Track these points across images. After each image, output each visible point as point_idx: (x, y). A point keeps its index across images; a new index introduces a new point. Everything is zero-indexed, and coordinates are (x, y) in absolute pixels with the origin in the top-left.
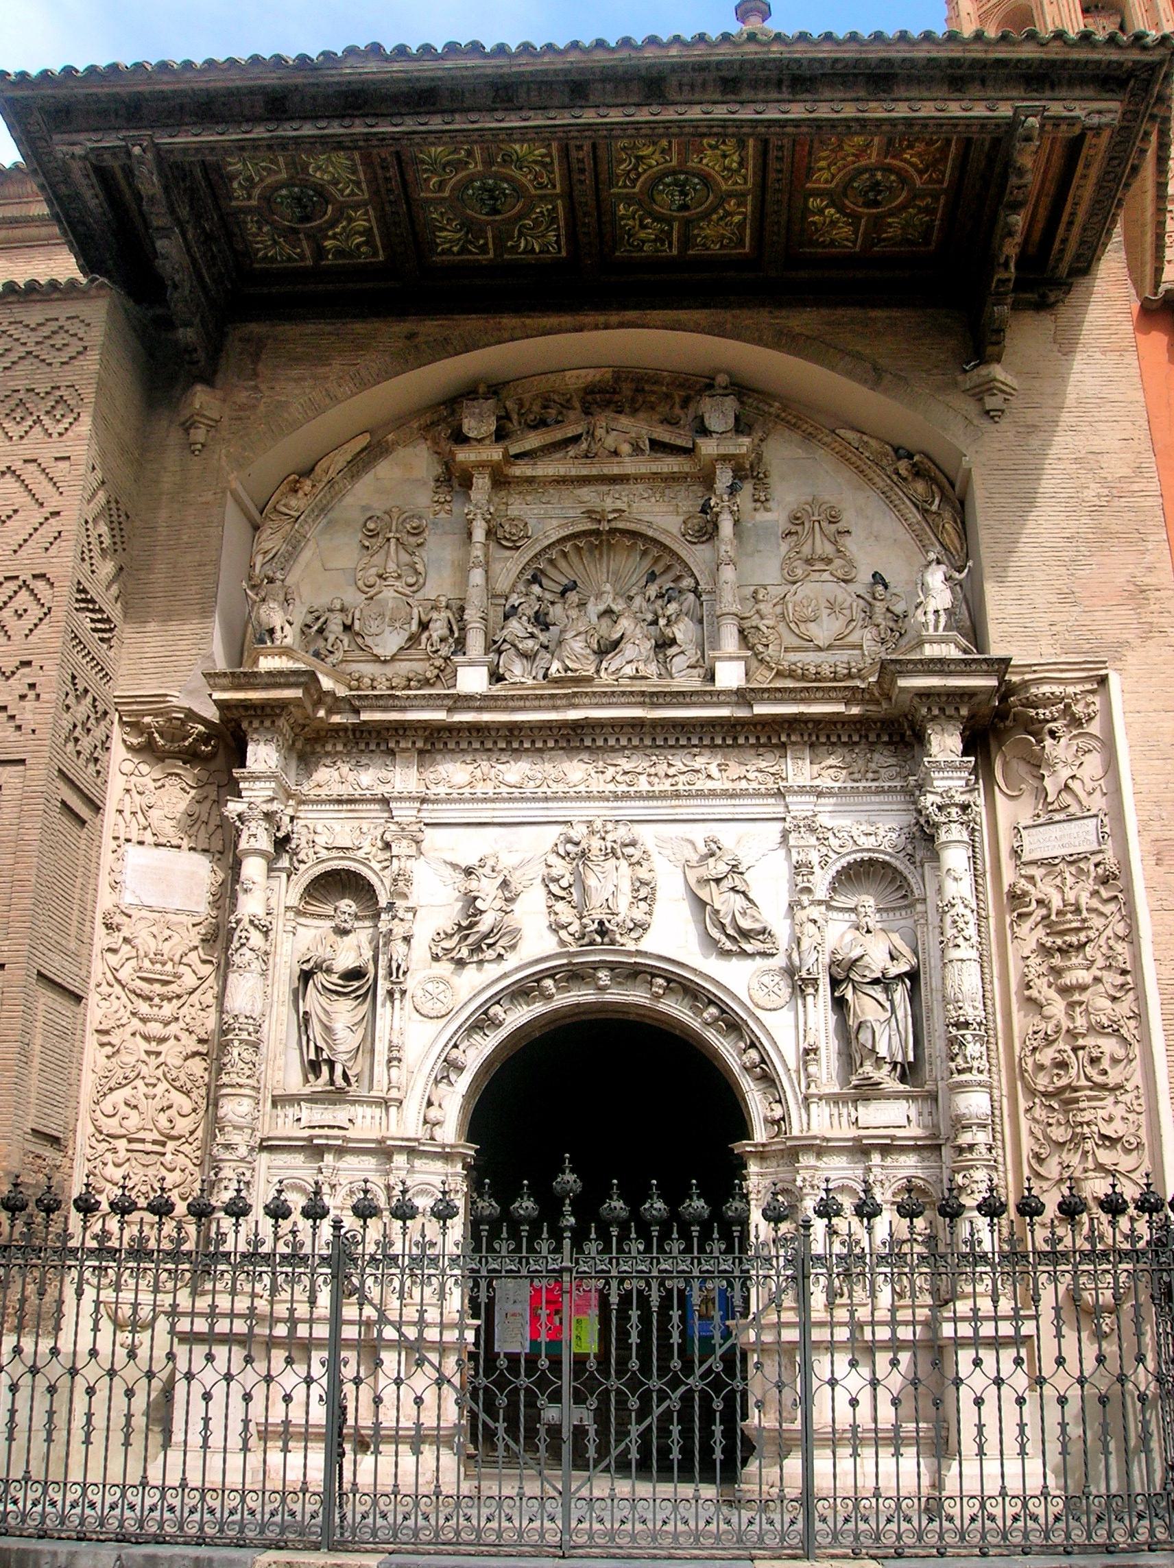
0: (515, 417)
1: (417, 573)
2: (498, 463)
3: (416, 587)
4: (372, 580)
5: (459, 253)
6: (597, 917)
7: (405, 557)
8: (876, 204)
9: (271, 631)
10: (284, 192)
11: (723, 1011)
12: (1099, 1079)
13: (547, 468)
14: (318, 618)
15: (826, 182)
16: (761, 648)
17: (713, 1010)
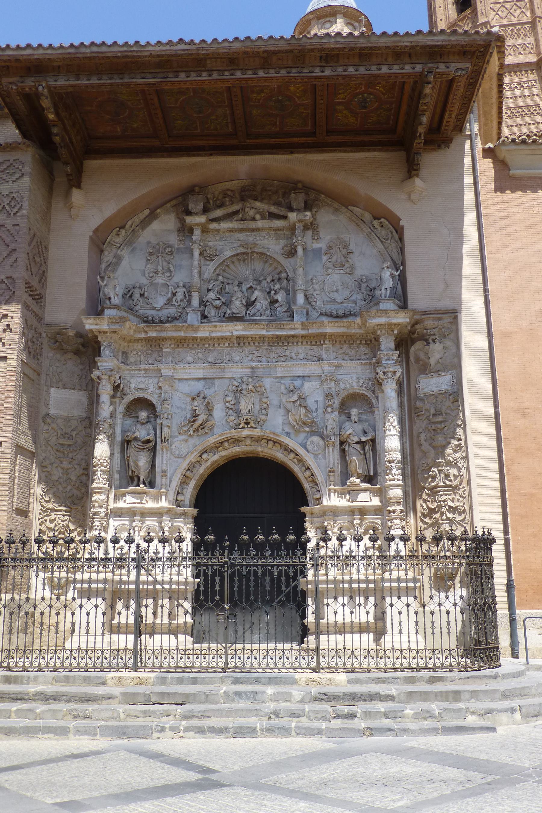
0: (211, 202)
1: (170, 271)
2: (204, 224)
3: (171, 277)
4: (151, 275)
6: (245, 417)
7: (165, 264)
8: (365, 107)
9: (110, 298)
11: (297, 455)
12: (448, 483)
13: (225, 225)
14: (129, 291)
15: (343, 99)
16: (314, 303)
17: (292, 455)
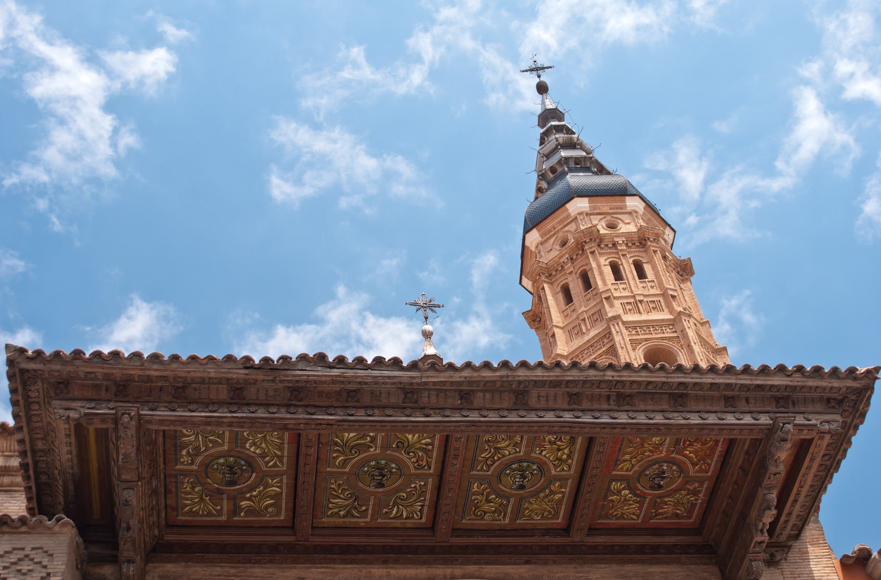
5: (344, 516)
8: (660, 487)
10: (222, 461)
15: (627, 470)
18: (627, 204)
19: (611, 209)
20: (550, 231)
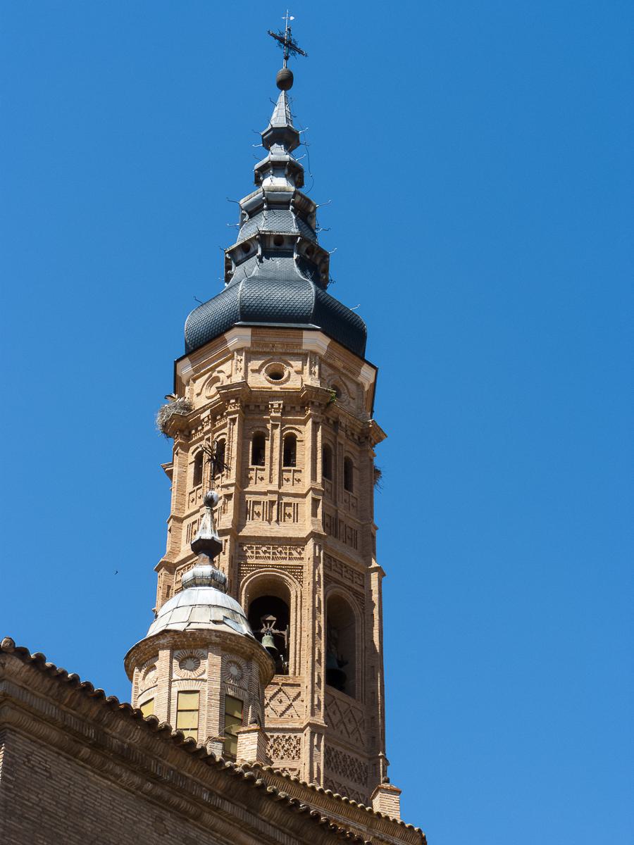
18: (362, 372)
19: (344, 367)
20: (266, 345)
